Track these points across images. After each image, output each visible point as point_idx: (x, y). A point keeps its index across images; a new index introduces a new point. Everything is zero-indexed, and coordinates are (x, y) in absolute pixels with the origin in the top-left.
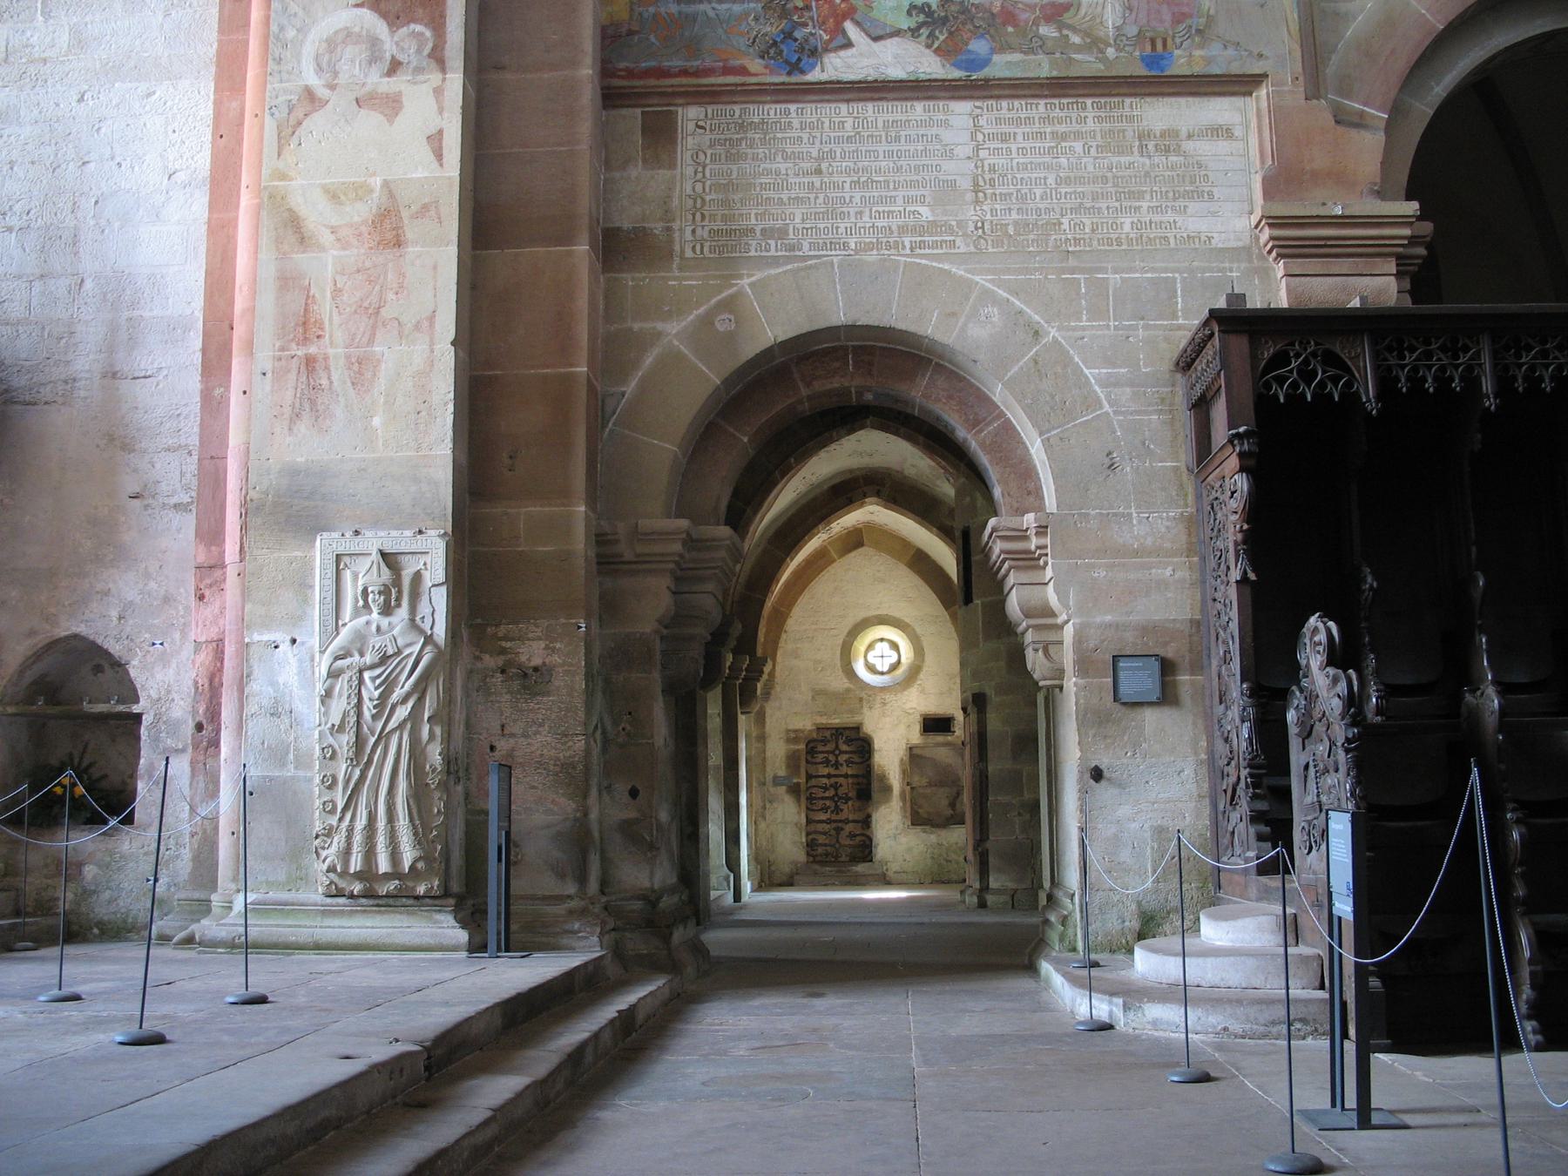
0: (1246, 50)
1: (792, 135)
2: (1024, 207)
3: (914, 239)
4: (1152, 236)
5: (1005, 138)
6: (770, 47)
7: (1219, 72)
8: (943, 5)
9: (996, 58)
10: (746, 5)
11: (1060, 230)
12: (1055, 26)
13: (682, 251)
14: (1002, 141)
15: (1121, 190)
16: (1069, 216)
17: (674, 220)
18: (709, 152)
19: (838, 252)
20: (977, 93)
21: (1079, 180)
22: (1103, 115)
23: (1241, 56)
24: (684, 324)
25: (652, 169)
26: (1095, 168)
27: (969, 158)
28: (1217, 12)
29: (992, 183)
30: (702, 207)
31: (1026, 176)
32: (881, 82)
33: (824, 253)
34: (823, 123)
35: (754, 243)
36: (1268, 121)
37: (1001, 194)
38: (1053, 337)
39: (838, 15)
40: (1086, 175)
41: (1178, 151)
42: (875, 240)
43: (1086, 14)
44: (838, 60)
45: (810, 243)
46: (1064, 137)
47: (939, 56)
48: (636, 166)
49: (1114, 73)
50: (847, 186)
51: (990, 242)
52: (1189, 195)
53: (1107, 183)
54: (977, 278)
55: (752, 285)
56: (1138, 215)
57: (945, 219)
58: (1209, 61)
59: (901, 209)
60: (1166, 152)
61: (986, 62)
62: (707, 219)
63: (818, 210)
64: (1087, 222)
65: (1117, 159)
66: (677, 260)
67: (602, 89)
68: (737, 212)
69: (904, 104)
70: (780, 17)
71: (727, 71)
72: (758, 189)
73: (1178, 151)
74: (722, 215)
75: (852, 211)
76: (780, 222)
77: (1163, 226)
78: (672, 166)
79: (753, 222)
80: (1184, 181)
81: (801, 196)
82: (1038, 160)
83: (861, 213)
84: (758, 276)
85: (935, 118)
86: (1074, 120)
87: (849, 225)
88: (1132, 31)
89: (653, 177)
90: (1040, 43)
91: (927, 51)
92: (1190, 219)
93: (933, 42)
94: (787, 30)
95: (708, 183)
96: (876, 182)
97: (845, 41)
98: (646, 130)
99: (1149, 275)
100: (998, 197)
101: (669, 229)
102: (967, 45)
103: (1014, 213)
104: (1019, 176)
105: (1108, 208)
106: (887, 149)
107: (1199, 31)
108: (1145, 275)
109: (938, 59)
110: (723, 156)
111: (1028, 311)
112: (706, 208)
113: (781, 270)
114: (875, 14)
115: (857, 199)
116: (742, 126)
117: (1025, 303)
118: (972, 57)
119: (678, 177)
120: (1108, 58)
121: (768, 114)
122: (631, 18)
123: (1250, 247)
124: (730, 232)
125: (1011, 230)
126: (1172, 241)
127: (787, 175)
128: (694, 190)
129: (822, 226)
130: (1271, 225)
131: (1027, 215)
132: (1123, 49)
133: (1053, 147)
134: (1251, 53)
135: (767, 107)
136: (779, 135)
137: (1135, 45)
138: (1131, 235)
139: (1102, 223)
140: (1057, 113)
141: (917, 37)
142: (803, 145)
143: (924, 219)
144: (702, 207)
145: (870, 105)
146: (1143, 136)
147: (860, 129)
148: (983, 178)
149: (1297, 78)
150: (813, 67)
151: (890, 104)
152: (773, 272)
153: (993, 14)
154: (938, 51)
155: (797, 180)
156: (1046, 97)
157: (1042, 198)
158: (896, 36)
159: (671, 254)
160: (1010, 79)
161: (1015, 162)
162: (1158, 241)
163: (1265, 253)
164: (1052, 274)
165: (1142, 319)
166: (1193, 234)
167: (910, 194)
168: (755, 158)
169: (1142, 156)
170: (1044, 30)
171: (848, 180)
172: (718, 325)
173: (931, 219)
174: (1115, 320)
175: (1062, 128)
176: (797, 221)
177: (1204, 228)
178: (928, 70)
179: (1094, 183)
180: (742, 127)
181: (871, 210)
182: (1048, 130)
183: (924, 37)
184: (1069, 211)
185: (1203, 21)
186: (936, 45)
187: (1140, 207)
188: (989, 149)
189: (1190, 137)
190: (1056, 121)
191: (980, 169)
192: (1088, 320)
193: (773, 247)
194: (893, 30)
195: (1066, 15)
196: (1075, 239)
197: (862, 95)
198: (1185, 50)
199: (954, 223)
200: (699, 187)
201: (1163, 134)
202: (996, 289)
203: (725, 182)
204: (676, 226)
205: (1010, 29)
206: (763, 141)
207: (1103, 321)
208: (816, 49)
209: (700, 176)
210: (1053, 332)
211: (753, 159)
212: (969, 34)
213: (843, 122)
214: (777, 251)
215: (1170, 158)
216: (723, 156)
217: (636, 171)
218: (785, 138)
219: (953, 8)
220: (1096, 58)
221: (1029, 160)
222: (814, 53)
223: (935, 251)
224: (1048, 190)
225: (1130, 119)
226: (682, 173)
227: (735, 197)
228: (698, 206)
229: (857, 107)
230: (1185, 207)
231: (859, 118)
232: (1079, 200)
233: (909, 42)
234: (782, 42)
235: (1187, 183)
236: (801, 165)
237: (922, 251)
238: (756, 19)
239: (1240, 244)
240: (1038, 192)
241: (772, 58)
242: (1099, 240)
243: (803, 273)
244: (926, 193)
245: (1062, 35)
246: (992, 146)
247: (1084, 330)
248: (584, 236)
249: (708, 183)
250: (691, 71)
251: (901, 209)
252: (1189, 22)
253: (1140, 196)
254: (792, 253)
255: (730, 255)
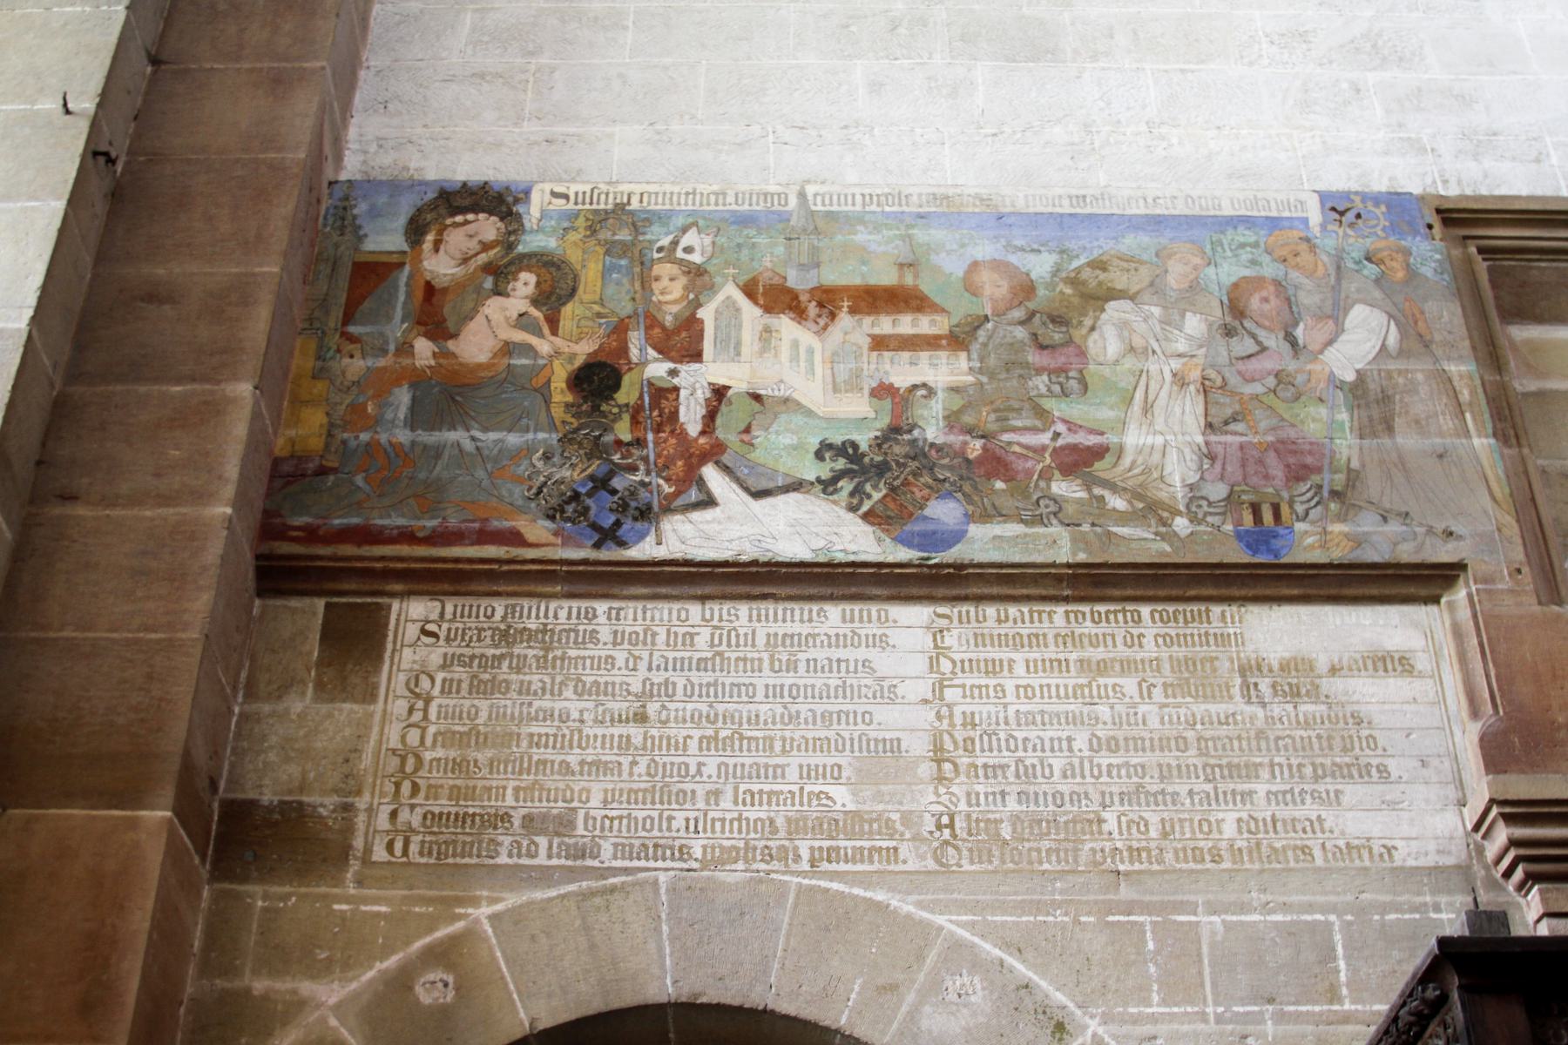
0: (1421, 525)
1: (597, 653)
2: (1032, 789)
3: (817, 844)
4: (1278, 845)
5: (993, 668)
6: (568, 502)
7: (1377, 559)
8: (879, 446)
9: (974, 530)
10: (530, 436)
11: (1100, 833)
12: (1079, 481)
13: (368, 850)
14: (987, 672)
15: (1212, 761)
16: (1117, 807)
17: (359, 793)
18: (439, 677)
19: (669, 864)
20: (941, 591)
21: (1138, 744)
22: (1173, 633)
23: (1415, 533)
24: (354, 985)
25: (332, 701)
26: (1162, 723)
27: (926, 701)
28: (1363, 466)
29: (969, 751)
30: (416, 770)
31: (1032, 735)
32: (768, 564)
33: (643, 863)
34: (654, 635)
35: (507, 840)
36: (1475, 641)
37: (985, 766)
38: (1095, 1035)
39: (691, 455)
40: (1147, 735)
41: (1315, 694)
42: (741, 844)
43: (1134, 462)
44: (688, 526)
45: (616, 845)
46: (1102, 668)
47: (872, 524)
48: (303, 694)
49: (1189, 559)
50: (693, 745)
51: (965, 853)
52: (1343, 772)
53: (1187, 749)
54: (940, 920)
55: (494, 918)
56: (1248, 806)
57: (880, 807)
58: (1358, 541)
59: (795, 788)
60: (1292, 696)
61: (958, 536)
62: (422, 794)
63: (635, 786)
64: (1154, 819)
65: (1203, 707)
66: (355, 866)
67: (258, 557)
68: (480, 784)
69: (807, 606)
70: (590, 456)
71: (485, 537)
72: (524, 744)
73: (1315, 694)
74: (452, 788)
75: (701, 791)
76: (560, 804)
77: (1299, 827)
78: (370, 696)
79: (510, 801)
80: (1331, 748)
81: (604, 758)
82: (1055, 708)
83: (717, 793)
84: (511, 900)
85: (863, 632)
86: (1119, 640)
87: (692, 815)
88: (1218, 491)
89: (330, 715)
90: (1053, 508)
91: (851, 515)
92: (1349, 815)
93: (861, 503)
94: (600, 475)
95: (432, 729)
96: (749, 739)
97: (702, 497)
98: (329, 634)
99: (1279, 917)
100: (981, 772)
101: (348, 808)
102: (921, 508)
103: (1012, 805)
104: (1020, 735)
105: (1191, 793)
106: (771, 682)
107: (1335, 494)
108: (1269, 918)
109: (869, 529)
110: (465, 686)
111: (1043, 984)
112: (420, 774)
113: (553, 893)
114: (757, 455)
115: (711, 768)
116: (505, 635)
117: (1033, 967)
118: (931, 527)
119: (377, 718)
120: (1175, 534)
121: (556, 617)
122: (327, 445)
123: (1469, 867)
124: (461, 819)
125: (1006, 832)
126: (1317, 853)
127: (582, 721)
128: (403, 738)
129: (641, 815)
130: (1509, 819)
131: (1037, 802)
132: (1203, 519)
133: (1082, 686)
134: (1430, 531)
135: (553, 605)
136: (572, 653)
137: (1224, 514)
138: (1239, 844)
139: (1180, 820)
140: (1088, 627)
141: (831, 494)
142: (615, 671)
143: (838, 807)
144: (416, 770)
145: (743, 609)
146: (1249, 670)
147: (724, 647)
148: (952, 736)
149: (1519, 571)
150: (642, 536)
151: (780, 607)
152: (539, 895)
153: (967, 460)
154: (866, 517)
155: (600, 731)
156: (1066, 600)
157: (1065, 776)
158: (794, 490)
159: (345, 852)
160: (1001, 566)
161: (1011, 710)
162: (1290, 853)
163: (1498, 876)
164: (1089, 914)
165: (1271, 1001)
166: (1356, 842)
167: (813, 761)
168: (524, 689)
169: (1249, 702)
170: (1061, 487)
171: (697, 734)
172: (419, 990)
173: (851, 807)
174: (1216, 1003)
175: (1098, 654)
176: (595, 801)
177: (1376, 832)
178: (852, 547)
179: (1162, 750)
180: (506, 636)
181: (736, 789)
182: (1073, 657)
183: (845, 493)
184: (1116, 799)
185: (1340, 478)
186: (865, 508)
187: (1251, 793)
188: (964, 686)
189: (1334, 671)
190: (1086, 641)
191: (946, 722)
192: (1164, 1002)
193: (543, 851)
194: (789, 481)
195: (1098, 465)
196: (1130, 848)
197: (730, 589)
198: (1313, 523)
199: (895, 817)
200: (413, 737)
201: (1285, 667)
202: (977, 940)
203: (465, 729)
204: (362, 803)
205: (999, 485)
206: (542, 663)
207: (1192, 1003)
208: (649, 508)
209: (417, 716)
210: (1093, 1026)
211: (520, 693)
212: (926, 491)
213: (692, 635)
214: (550, 857)
215: (1303, 708)
216: (465, 686)
217: (297, 704)
218: (584, 658)
219: (897, 449)
220: (1156, 534)
221: (1040, 707)
222: (645, 514)
223: (859, 867)
224: (1076, 762)
225: (1222, 639)
226: (385, 711)
227: (479, 756)
228: (409, 768)
229: (719, 610)
230: (1337, 792)
231: (722, 628)
232: (1135, 779)
233: (818, 502)
234: (590, 494)
235: (1337, 750)
236: (610, 705)
237: (834, 867)
238: (547, 457)
239: (1450, 861)
240: (1058, 764)
241: (568, 519)
242: (1176, 852)
243: (598, 901)
244: (843, 761)
245: (1093, 497)
246: (969, 682)
247: (1156, 1021)
248: (168, 793)
249: (432, 729)
250: (420, 535)
251: (795, 788)
252: (1316, 479)
253: (1251, 771)
254: (579, 863)
255: (458, 860)
